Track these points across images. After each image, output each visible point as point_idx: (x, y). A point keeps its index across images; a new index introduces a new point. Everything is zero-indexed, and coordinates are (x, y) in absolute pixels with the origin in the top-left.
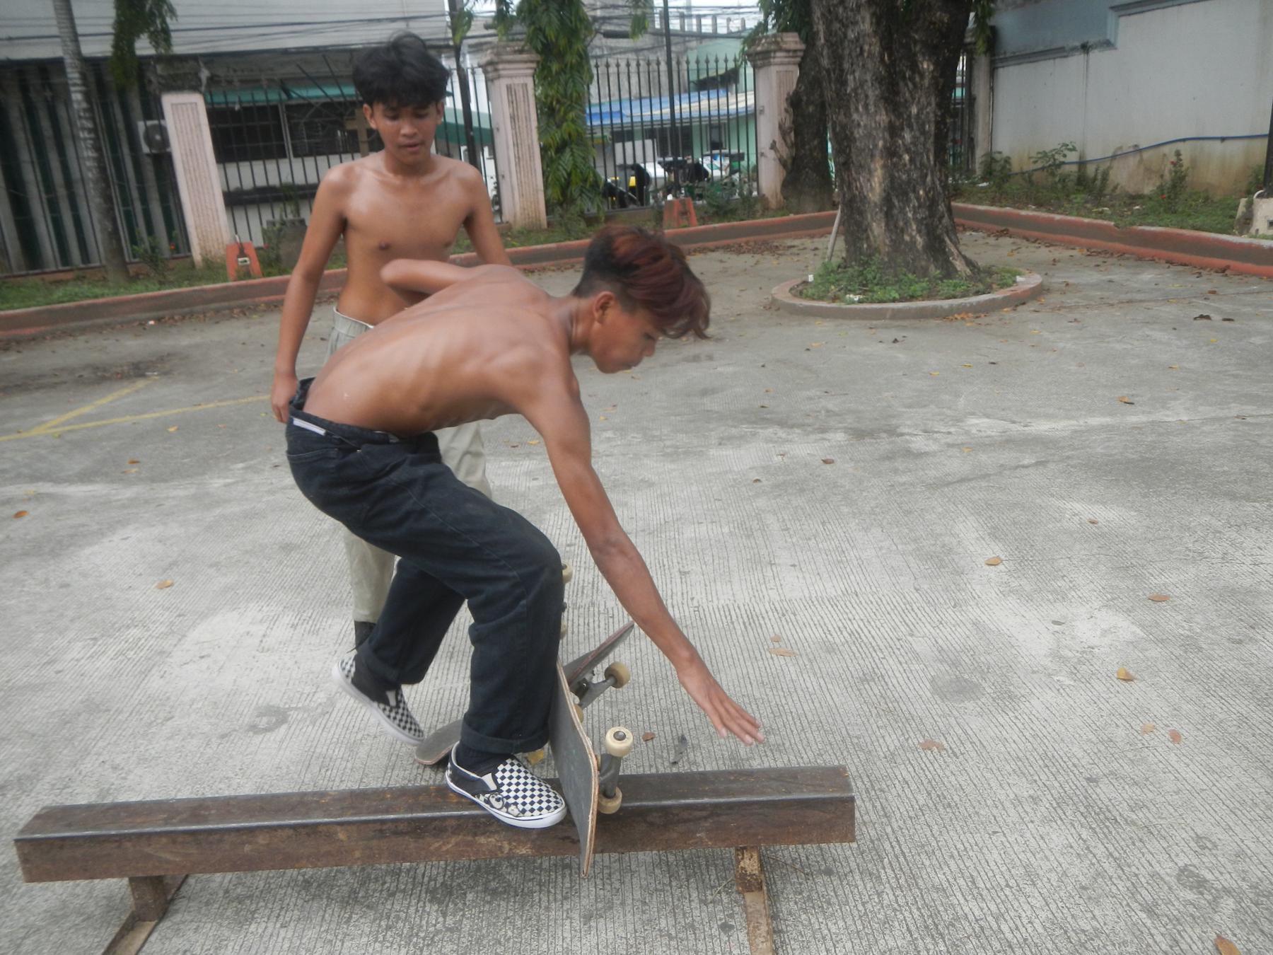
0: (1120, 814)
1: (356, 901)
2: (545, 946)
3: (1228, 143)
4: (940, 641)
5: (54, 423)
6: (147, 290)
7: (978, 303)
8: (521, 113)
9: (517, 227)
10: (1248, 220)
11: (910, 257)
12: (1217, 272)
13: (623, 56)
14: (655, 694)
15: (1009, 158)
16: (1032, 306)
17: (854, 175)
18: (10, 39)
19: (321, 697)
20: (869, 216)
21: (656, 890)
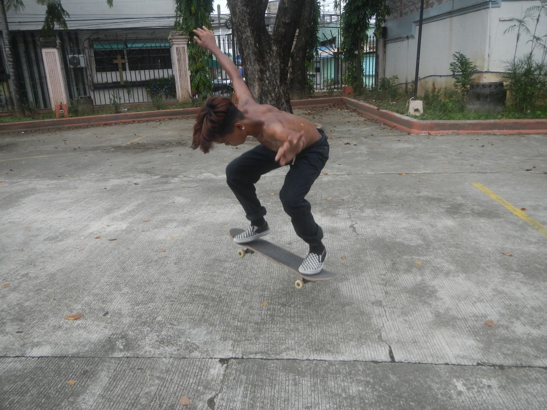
3: (442, 77)
8: (182, 58)
9: (180, 102)
18: (20, 22)
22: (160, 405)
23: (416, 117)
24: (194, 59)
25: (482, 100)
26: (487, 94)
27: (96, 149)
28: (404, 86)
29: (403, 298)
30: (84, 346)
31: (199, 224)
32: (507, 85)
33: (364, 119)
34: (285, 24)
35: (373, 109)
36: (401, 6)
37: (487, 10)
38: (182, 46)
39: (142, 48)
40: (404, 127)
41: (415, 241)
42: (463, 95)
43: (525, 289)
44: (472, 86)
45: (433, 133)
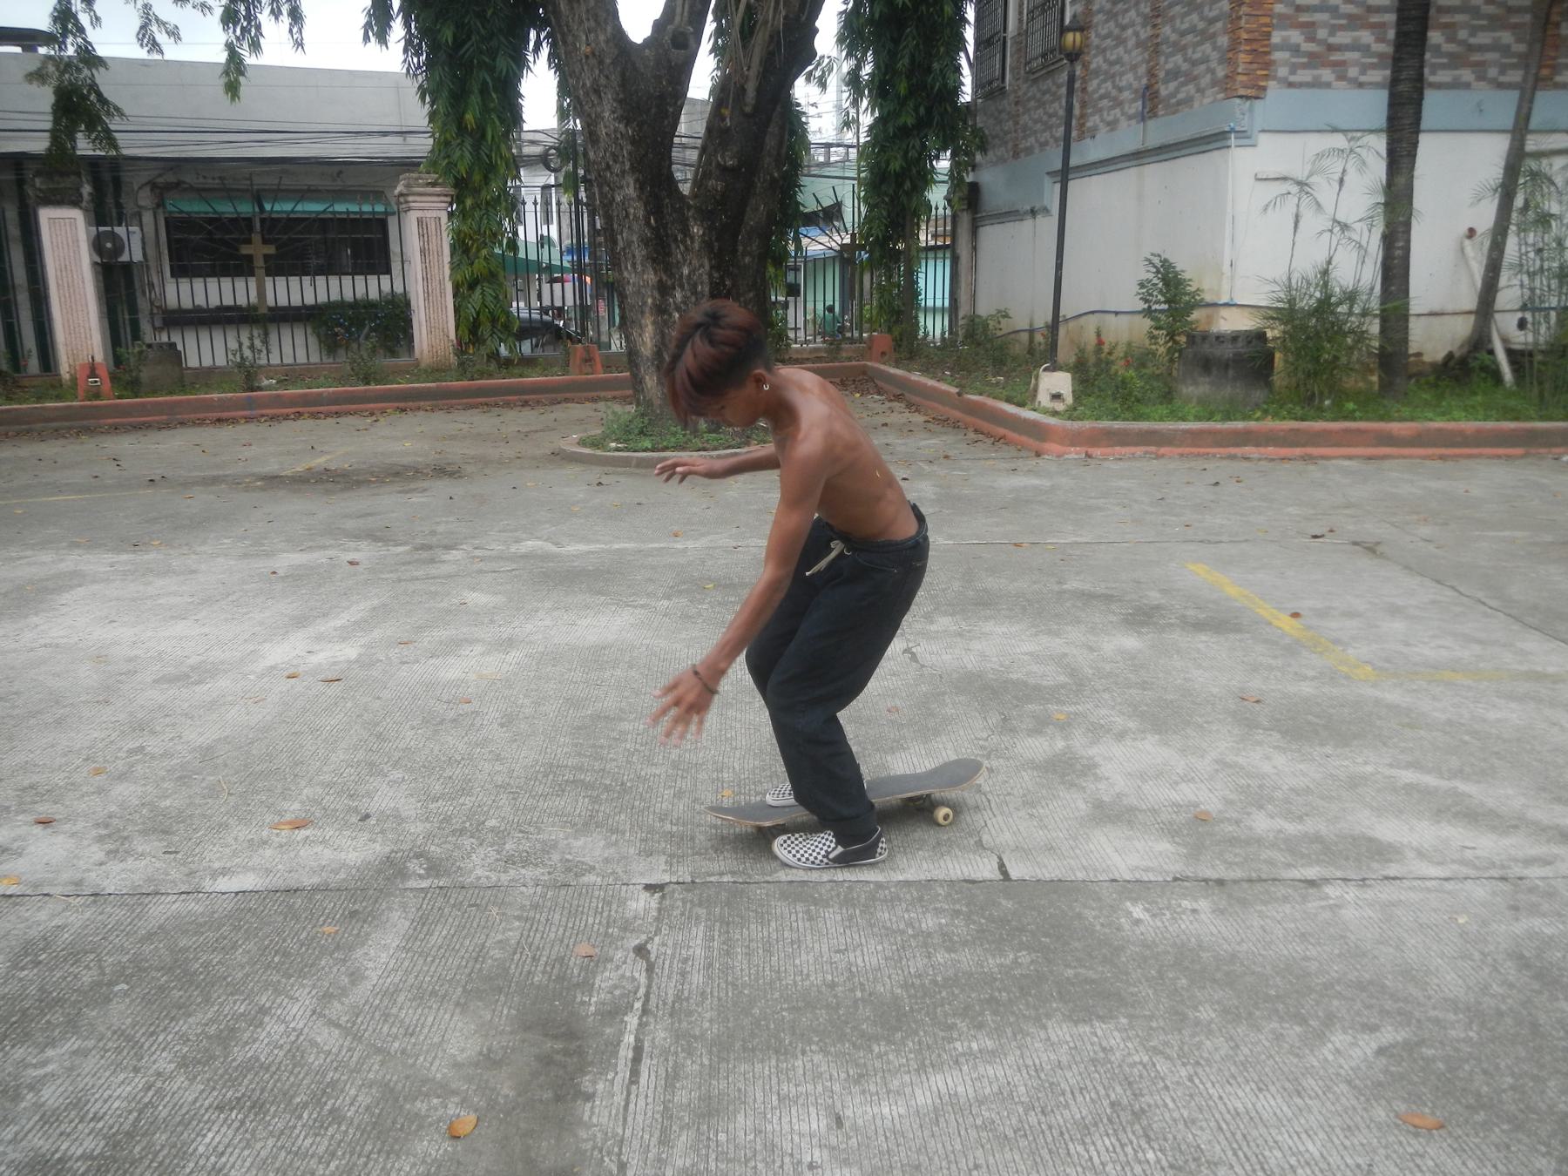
3: (1119, 316)
8: (433, 246)
9: (423, 365)
10: (1036, 390)
22: (534, 958)
23: (1055, 413)
24: (466, 251)
25: (1215, 371)
26: (1228, 360)
27: (215, 480)
28: (1025, 337)
29: (1026, 778)
30: (336, 872)
31: (541, 649)
32: (1275, 339)
33: (926, 418)
34: (724, 169)
35: (947, 393)
36: (1016, 131)
37: (1225, 151)
38: (434, 214)
39: (322, 216)
40: (1024, 439)
41: (1052, 676)
42: (1171, 360)
43: (1280, 760)
44: (1192, 339)
45: (1097, 452)
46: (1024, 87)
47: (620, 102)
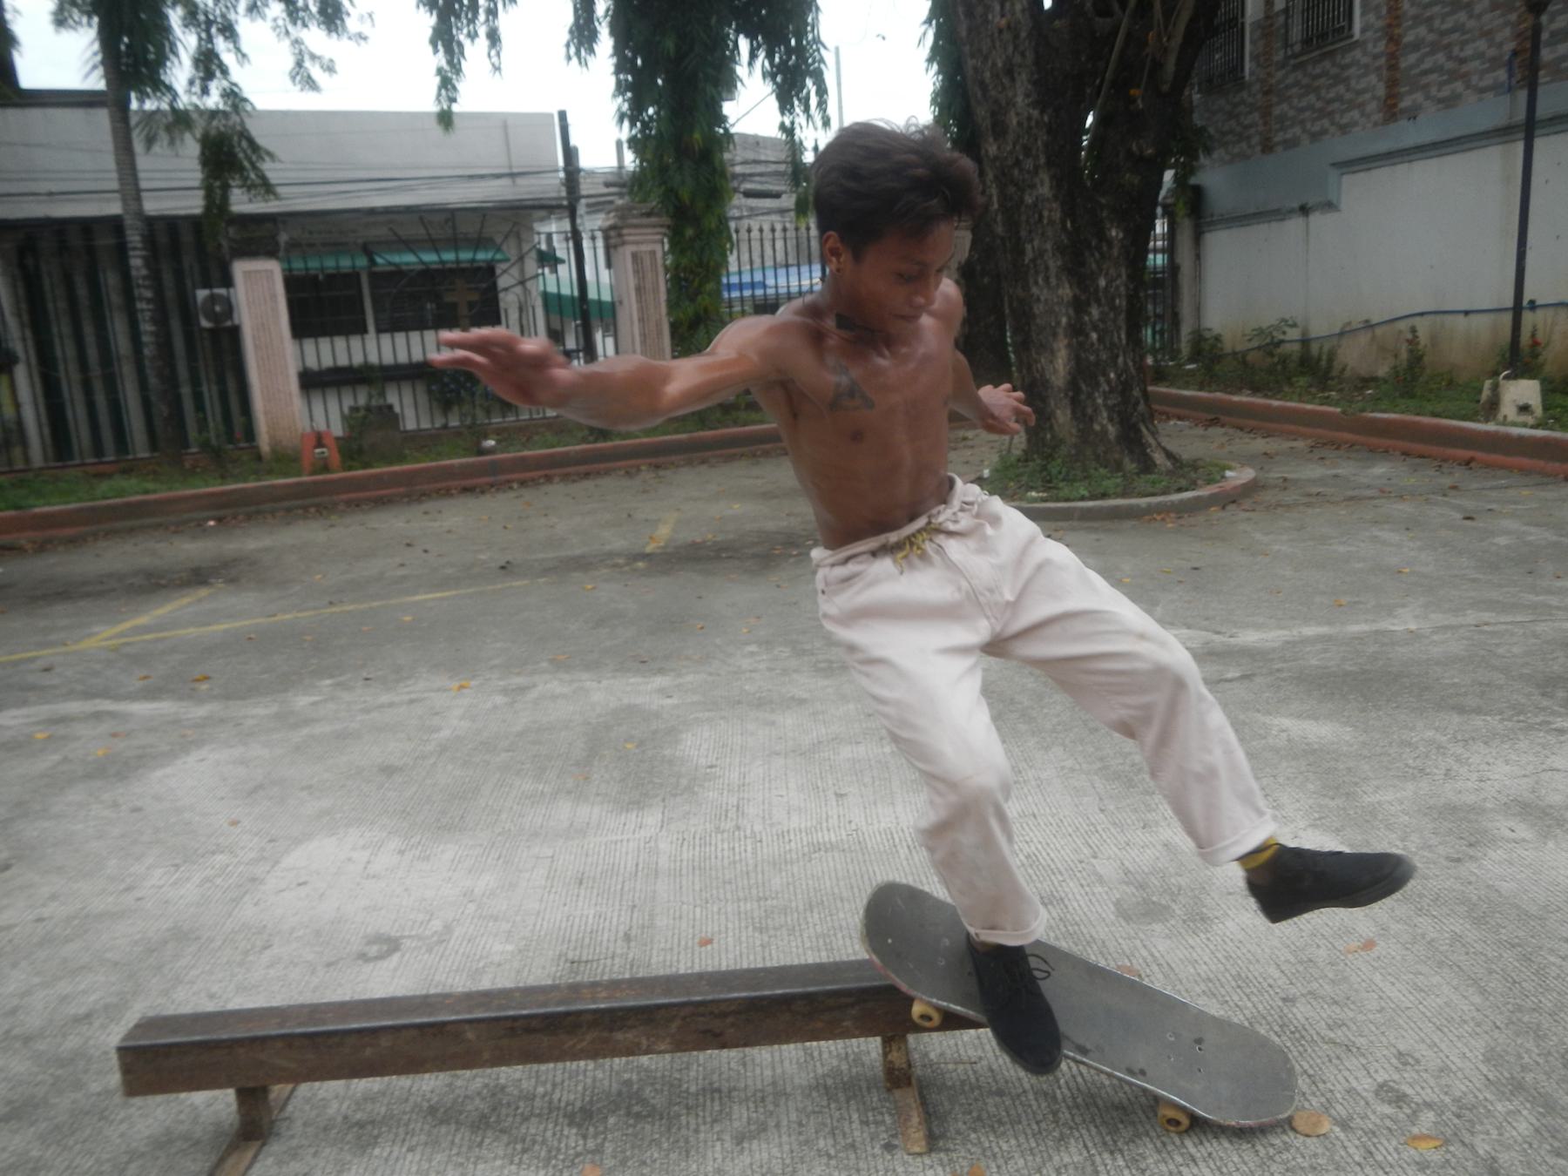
0: (1318, 1034)
1: (488, 1126)
2: (694, 1167)
3: (1472, 317)
4: (1126, 863)
5: (105, 635)
6: (207, 485)
7: (1181, 501)
10: (1493, 405)
11: (1101, 449)
12: (1460, 464)
13: (765, 218)
14: (810, 920)
15: (1220, 335)
16: (1247, 504)
17: (1034, 356)
18: (51, 194)
19: (437, 925)
20: (1052, 403)
21: (814, 1112)
23: (1525, 425)
40: (1525, 461)
46: (1280, 74)
47: (1035, 83)
